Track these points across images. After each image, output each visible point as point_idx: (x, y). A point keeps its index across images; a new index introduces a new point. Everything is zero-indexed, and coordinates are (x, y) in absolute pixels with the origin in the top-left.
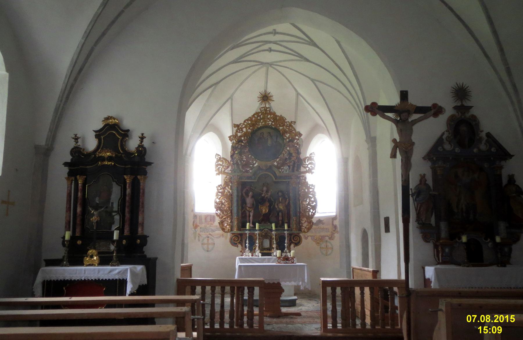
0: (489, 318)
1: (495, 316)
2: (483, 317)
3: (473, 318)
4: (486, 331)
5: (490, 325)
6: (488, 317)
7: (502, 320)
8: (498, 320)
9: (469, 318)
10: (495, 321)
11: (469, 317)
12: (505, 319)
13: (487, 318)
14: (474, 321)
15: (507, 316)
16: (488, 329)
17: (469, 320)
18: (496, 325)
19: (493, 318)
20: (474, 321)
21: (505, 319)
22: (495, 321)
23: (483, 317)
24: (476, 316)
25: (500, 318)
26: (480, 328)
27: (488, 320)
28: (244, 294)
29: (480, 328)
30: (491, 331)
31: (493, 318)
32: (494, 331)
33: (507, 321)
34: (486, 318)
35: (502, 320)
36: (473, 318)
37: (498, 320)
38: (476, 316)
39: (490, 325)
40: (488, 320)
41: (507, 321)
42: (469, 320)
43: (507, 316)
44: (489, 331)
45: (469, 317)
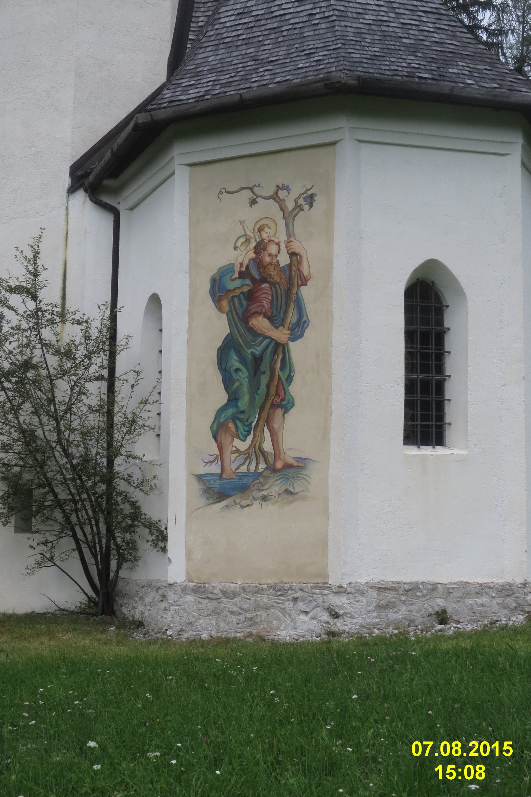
0: (458, 748)
1: (471, 744)
2: (445, 746)
3: (425, 747)
4: (451, 774)
5: (460, 762)
6: (457, 745)
7: (485, 752)
8: (478, 751)
9: (417, 749)
10: (472, 754)
11: (417, 746)
12: (492, 751)
13: (455, 748)
14: (427, 754)
15: (496, 744)
16: (456, 770)
17: (417, 752)
18: (474, 761)
19: (466, 749)
20: (427, 754)
21: (492, 751)
22: (472, 754)
23: (445, 746)
24: (431, 743)
25: (479, 747)
26: (440, 768)
27: (457, 752)
28: (92, 510)
29: (440, 768)
30: (462, 774)
31: (466, 749)
32: (469, 775)
33: (497, 754)
34: (452, 748)
35: (485, 752)
36: (425, 747)
37: (478, 751)
38: (431, 743)
39: (460, 762)
40: (457, 752)
41: (497, 754)
42: (417, 752)
43: (496, 744)
44: (458, 774)
45: (417, 746)
